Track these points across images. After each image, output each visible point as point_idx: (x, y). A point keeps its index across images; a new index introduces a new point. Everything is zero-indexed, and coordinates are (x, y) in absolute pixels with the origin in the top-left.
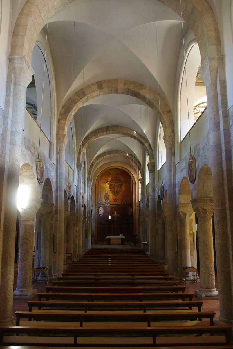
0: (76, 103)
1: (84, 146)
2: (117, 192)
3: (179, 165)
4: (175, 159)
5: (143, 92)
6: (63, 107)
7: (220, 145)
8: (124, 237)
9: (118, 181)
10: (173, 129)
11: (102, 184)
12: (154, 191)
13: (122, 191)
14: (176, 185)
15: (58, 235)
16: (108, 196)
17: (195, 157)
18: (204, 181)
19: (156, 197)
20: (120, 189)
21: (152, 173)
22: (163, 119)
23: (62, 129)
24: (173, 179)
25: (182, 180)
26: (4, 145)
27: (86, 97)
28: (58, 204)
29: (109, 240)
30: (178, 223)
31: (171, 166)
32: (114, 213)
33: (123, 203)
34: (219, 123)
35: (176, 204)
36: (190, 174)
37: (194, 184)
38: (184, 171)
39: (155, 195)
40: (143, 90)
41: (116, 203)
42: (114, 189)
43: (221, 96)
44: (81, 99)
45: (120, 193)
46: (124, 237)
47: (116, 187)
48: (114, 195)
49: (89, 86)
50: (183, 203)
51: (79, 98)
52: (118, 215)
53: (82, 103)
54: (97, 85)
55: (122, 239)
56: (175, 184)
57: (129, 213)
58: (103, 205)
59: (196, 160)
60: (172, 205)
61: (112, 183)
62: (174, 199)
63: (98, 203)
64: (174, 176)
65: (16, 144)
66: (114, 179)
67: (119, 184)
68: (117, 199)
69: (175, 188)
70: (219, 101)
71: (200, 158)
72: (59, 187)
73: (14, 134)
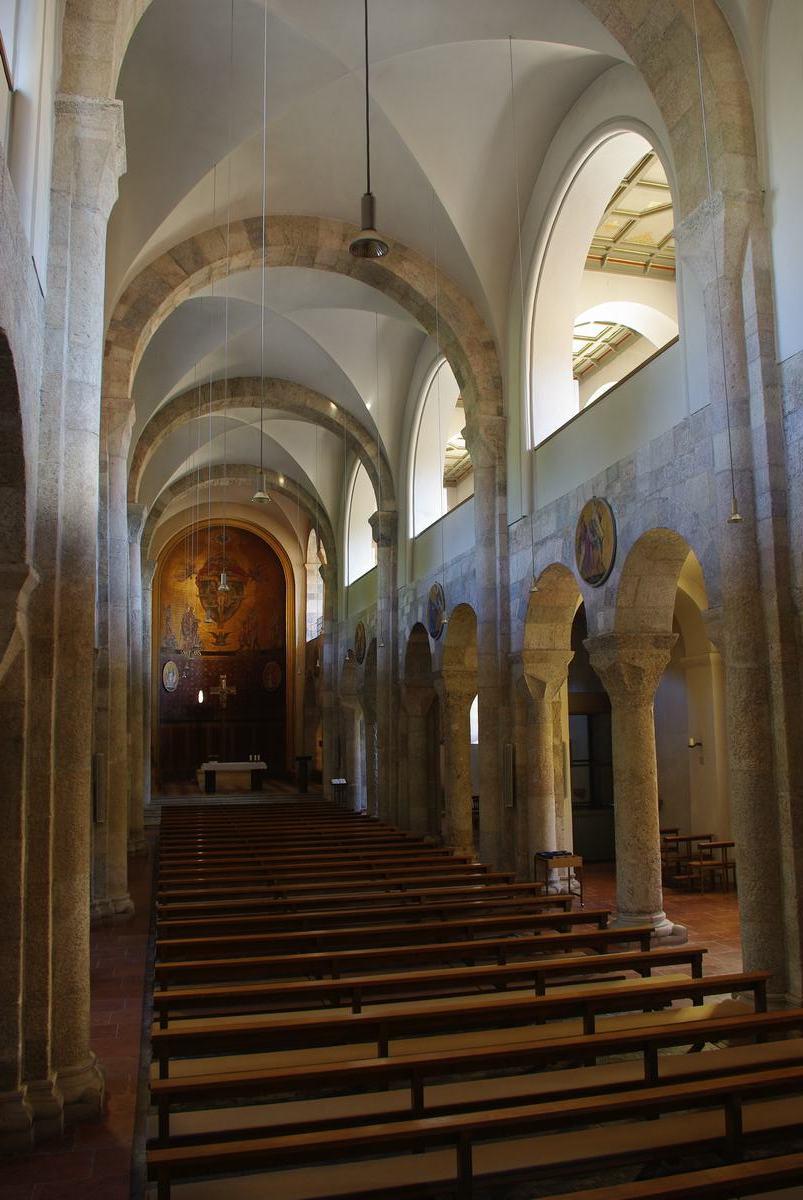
0: (172, 288)
1: (149, 446)
2: (226, 610)
3: (525, 523)
4: (505, 504)
5: (406, 272)
6: (124, 299)
7: (751, 472)
8: (263, 766)
10: (500, 404)
11: (172, 582)
12: (395, 607)
13: (242, 607)
14: (508, 592)
15: (109, 763)
17: (609, 501)
18: (639, 580)
19: (401, 628)
21: (387, 549)
22: (469, 371)
23: (119, 381)
24: (501, 570)
25: (542, 573)
26: (50, 431)
27: (206, 269)
28: (107, 649)
29: (210, 775)
30: (518, 716)
31: (492, 529)
32: (217, 683)
33: (246, 648)
34: (746, 401)
35: (509, 652)
36: (587, 557)
37: (604, 588)
38: (549, 544)
39: (396, 621)
40: (406, 265)
41: (224, 649)
43: (758, 317)
44: (188, 274)
45: (237, 613)
46: (263, 766)
49: (218, 232)
50: (536, 647)
51: (184, 274)
52: (233, 691)
53: (188, 289)
54: (248, 232)
55: (255, 773)
56: (505, 587)
57: (270, 682)
59: (615, 511)
60: (496, 655)
62: (502, 634)
63: (163, 650)
64: (505, 559)
65: (86, 430)
69: (506, 598)
70: (747, 334)
71: (639, 505)
72: (109, 589)
73: (81, 390)
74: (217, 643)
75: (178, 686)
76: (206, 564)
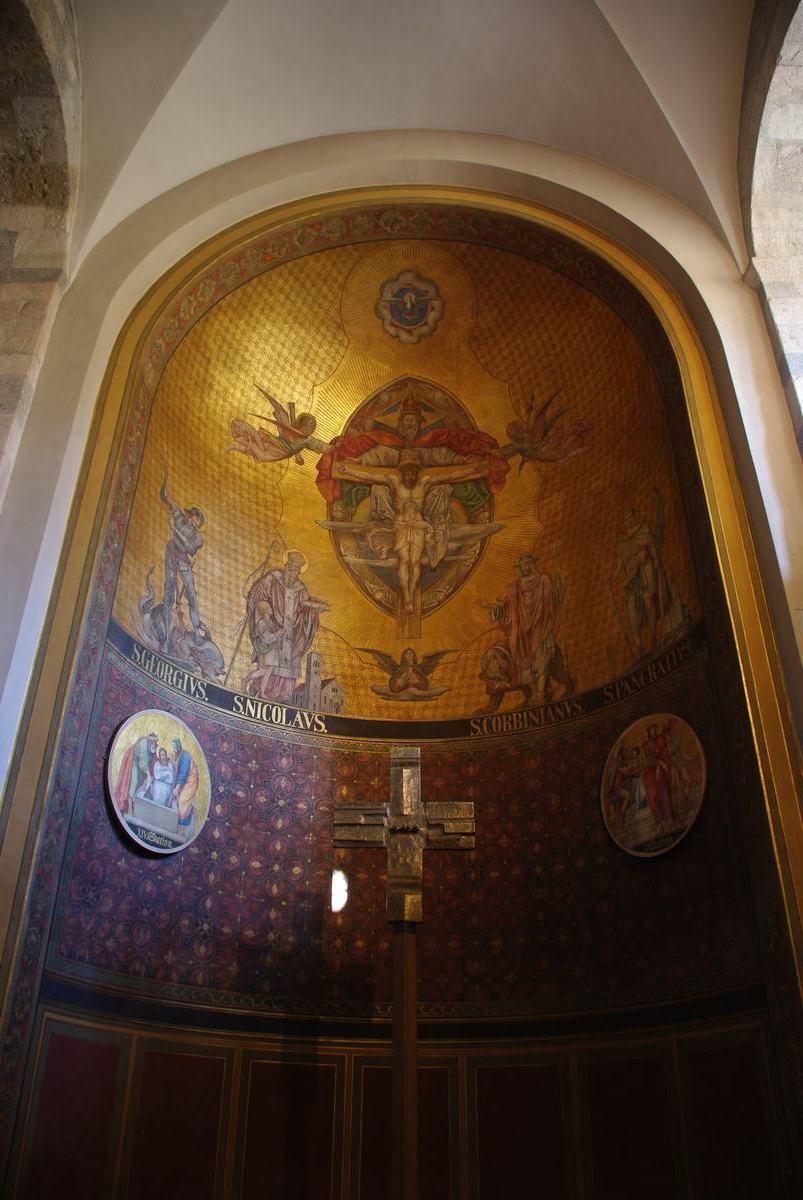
2: (429, 576)
9: (434, 443)
16: (303, 611)
20: (462, 538)
33: (512, 701)
41: (421, 712)
42: (393, 537)
45: (470, 586)
47: (411, 516)
48: (388, 609)
52: (461, 818)
58: (205, 706)
61: (361, 474)
66: (392, 420)
67: (451, 482)
68: (433, 659)
74: (394, 692)
75: (204, 840)
76: (355, 421)
